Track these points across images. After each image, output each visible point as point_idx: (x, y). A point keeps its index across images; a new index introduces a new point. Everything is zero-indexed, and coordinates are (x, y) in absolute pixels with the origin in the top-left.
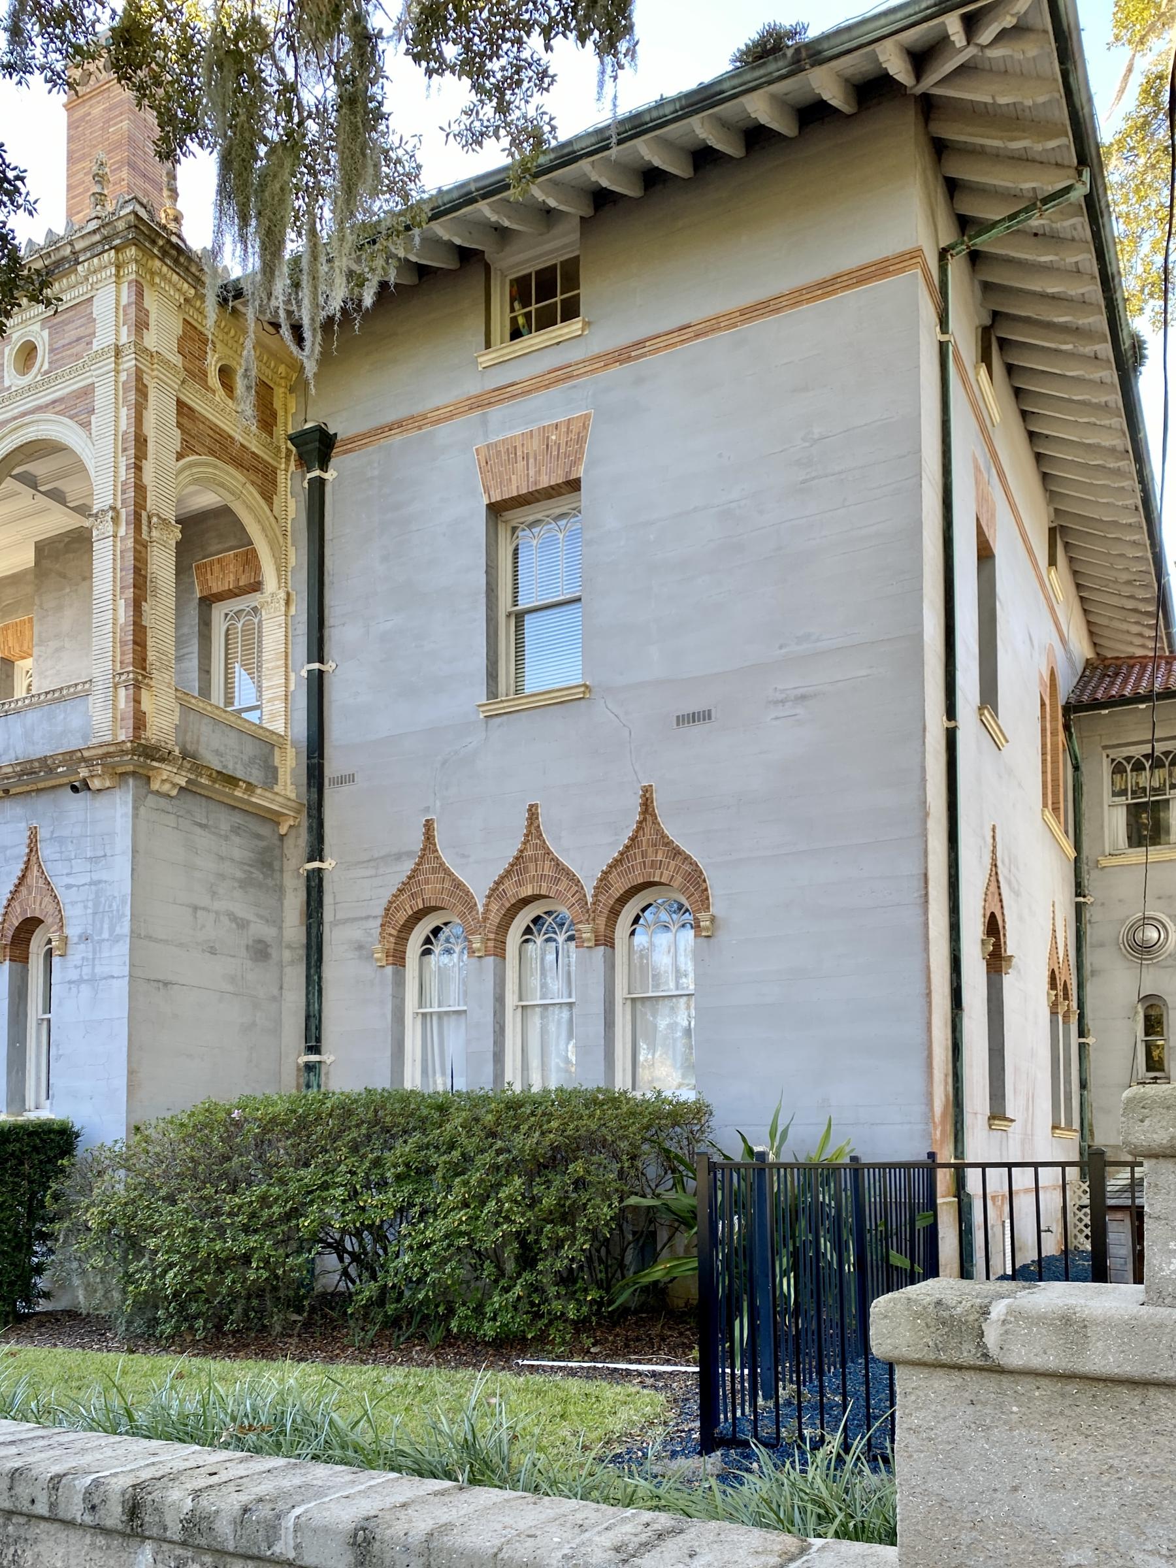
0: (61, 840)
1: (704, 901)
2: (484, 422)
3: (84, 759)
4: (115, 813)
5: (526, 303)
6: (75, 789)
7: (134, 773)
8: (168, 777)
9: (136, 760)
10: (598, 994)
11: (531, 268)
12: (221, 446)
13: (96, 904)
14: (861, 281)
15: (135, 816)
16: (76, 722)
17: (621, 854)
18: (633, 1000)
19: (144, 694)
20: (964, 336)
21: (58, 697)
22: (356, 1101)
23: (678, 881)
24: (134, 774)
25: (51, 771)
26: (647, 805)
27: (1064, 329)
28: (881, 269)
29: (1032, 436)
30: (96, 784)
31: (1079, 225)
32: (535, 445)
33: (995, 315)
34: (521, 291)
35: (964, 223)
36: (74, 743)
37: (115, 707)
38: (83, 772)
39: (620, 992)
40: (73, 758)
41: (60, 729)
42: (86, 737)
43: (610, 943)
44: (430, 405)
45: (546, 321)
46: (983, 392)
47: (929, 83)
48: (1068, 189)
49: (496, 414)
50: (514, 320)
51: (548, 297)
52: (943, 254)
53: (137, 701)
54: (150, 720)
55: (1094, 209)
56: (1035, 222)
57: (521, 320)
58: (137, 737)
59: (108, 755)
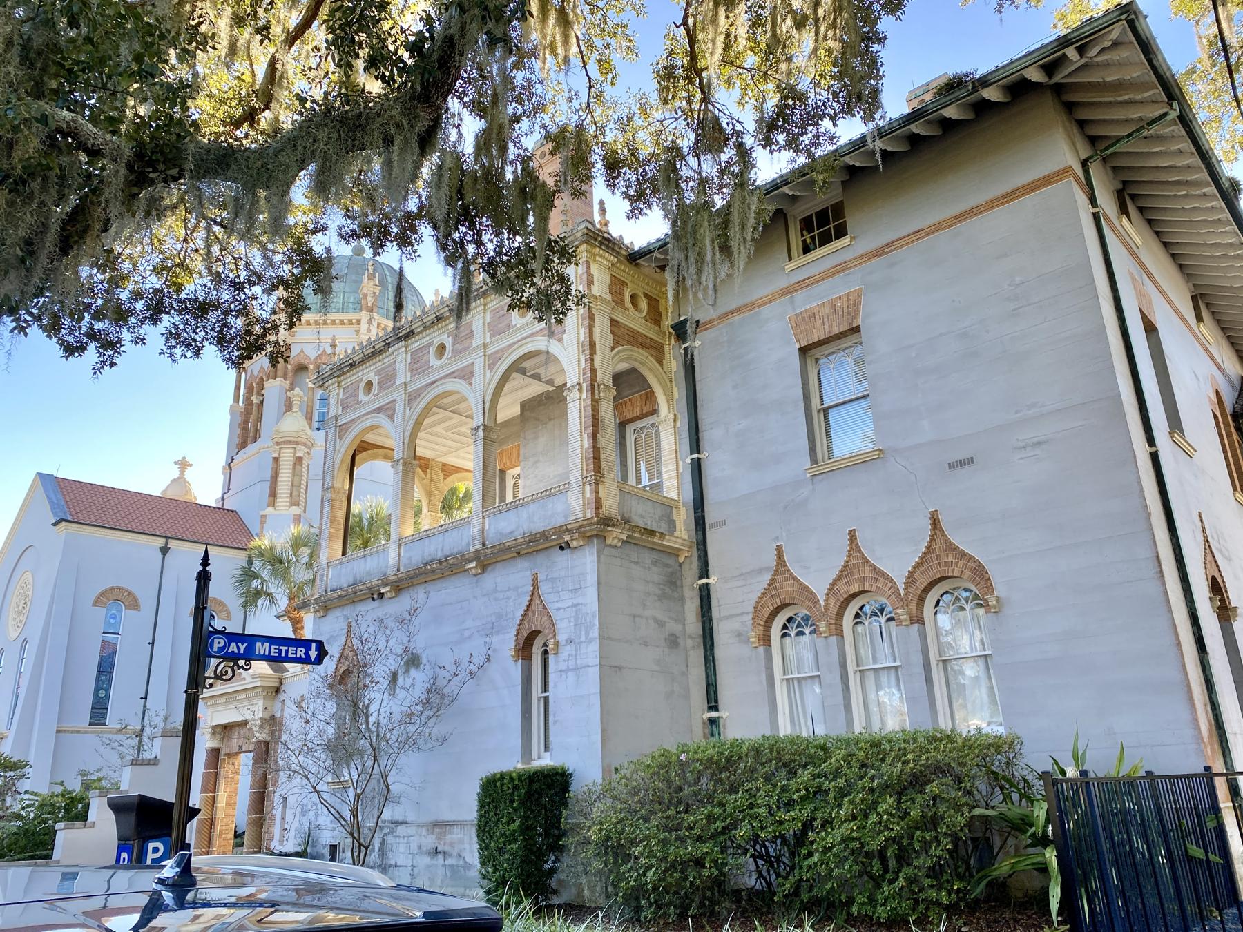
0: (553, 580)
1: (990, 588)
2: (792, 302)
3: (567, 530)
4: (586, 562)
5: (811, 230)
6: (562, 548)
7: (597, 536)
8: (616, 535)
9: (598, 528)
10: (917, 658)
11: (812, 212)
12: (636, 339)
13: (577, 618)
14: (1031, 191)
15: (598, 561)
16: (560, 507)
17: (921, 558)
18: (944, 661)
19: (600, 487)
20: (1107, 203)
21: (548, 494)
22: (761, 745)
23: (967, 574)
24: (597, 536)
25: (547, 539)
26: (935, 523)
27: (1178, 183)
28: (1046, 181)
29: (1166, 244)
30: (574, 544)
31: (1179, 130)
32: (827, 310)
33: (1125, 183)
34: (807, 224)
35: (1093, 140)
36: (559, 521)
37: (584, 497)
38: (567, 538)
39: (934, 657)
40: (561, 530)
41: (550, 513)
42: (566, 517)
43: (921, 621)
44: (756, 297)
45: (825, 240)
46: (1129, 233)
47: (1058, 78)
48: (1165, 114)
49: (799, 296)
50: (804, 241)
51: (825, 227)
52: (1084, 164)
53: (597, 492)
54: (604, 503)
55: (1186, 121)
56: (1145, 133)
57: (808, 241)
58: (597, 514)
59: (582, 526)
